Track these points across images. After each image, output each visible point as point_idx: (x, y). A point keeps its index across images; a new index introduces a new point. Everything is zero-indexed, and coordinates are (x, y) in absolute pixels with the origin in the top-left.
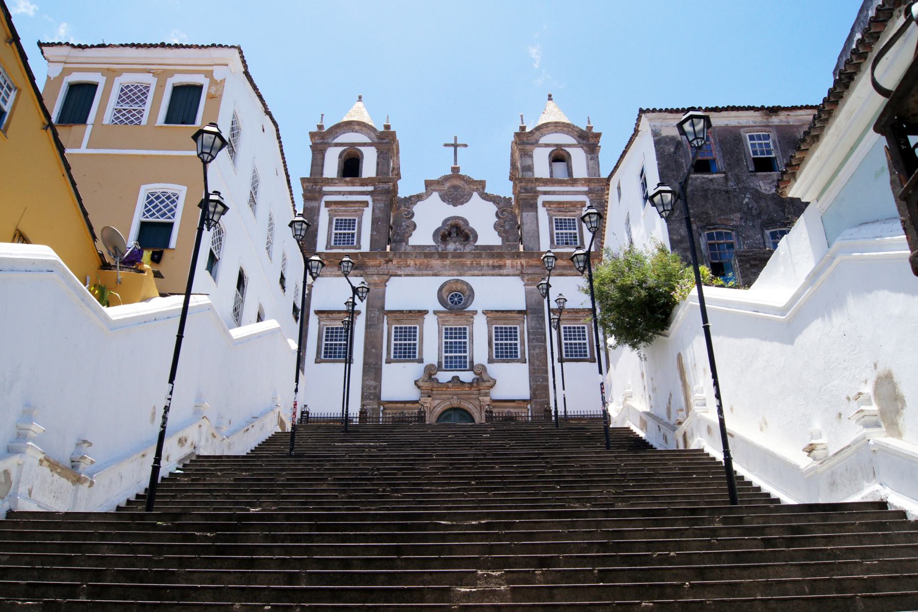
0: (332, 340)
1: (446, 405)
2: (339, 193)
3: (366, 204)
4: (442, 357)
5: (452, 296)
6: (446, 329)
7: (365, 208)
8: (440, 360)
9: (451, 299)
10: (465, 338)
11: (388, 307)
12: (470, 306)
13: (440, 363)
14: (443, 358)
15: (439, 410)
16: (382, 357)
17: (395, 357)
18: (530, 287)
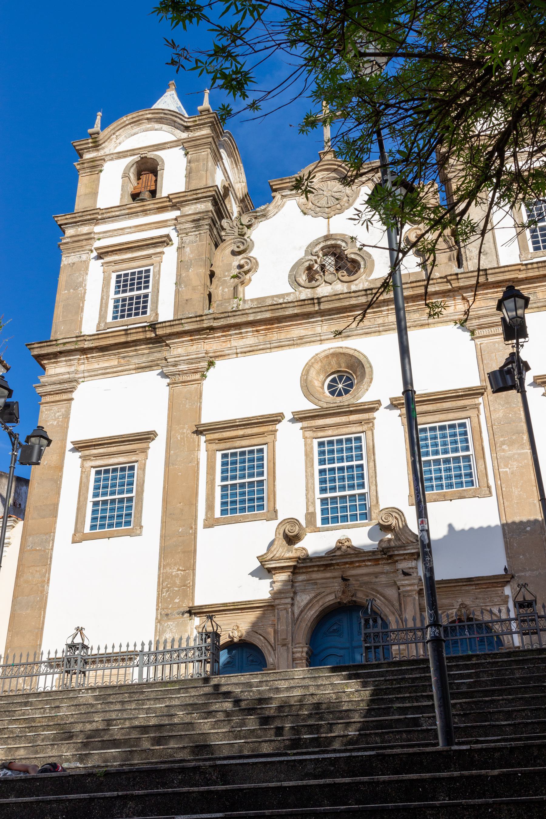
0: (105, 494)
1: (330, 599)
2: (122, 231)
3: (165, 241)
4: (314, 503)
5: (333, 380)
6: (321, 444)
7: (166, 250)
8: (311, 510)
9: (330, 387)
10: (360, 457)
11: (207, 418)
12: (368, 393)
13: (310, 516)
14: (318, 503)
15: (312, 613)
16: (196, 516)
17: (224, 512)
18: (485, 341)
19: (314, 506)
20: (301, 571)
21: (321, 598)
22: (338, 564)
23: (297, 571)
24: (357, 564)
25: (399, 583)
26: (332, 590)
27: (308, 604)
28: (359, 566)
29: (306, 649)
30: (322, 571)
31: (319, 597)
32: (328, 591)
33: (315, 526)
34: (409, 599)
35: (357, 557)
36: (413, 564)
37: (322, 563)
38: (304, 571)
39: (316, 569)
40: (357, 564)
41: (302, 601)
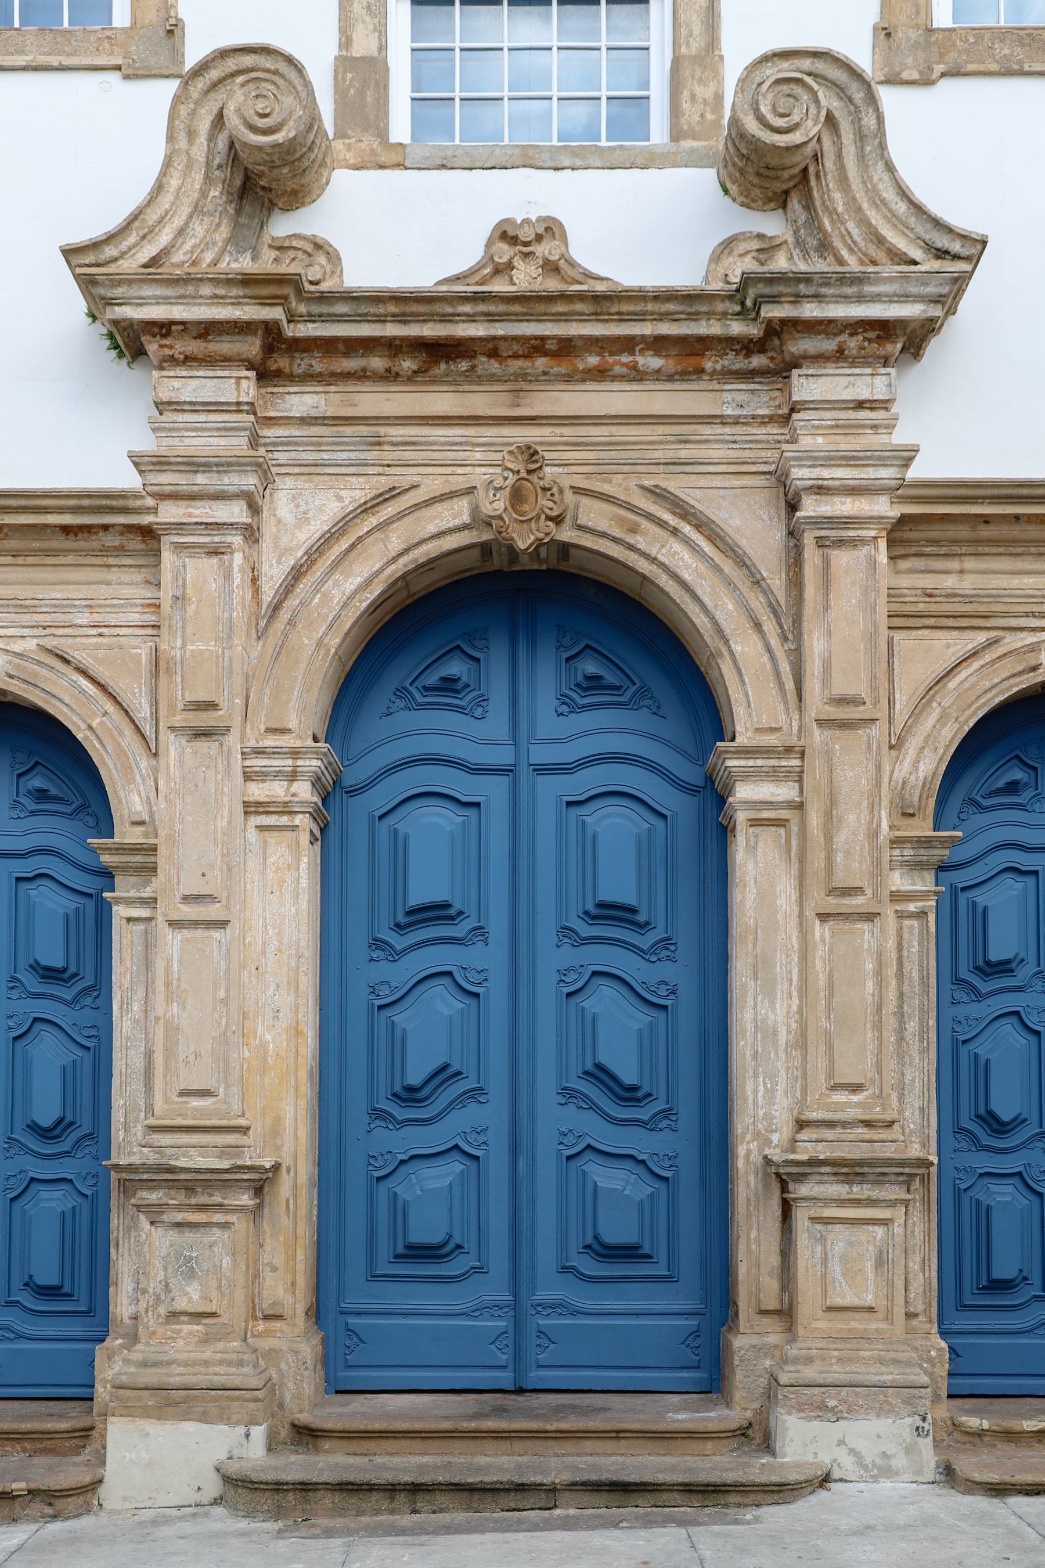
19: (381, 31)
20: (301, 364)
21: (401, 516)
22: (493, 348)
23: (282, 362)
24: (593, 360)
25: (801, 474)
26: (459, 483)
27: (329, 538)
28: (601, 374)
29: (312, 764)
30: (412, 378)
31: (388, 510)
32: (433, 484)
33: (382, 134)
34: (841, 558)
35: (597, 316)
36: (880, 382)
37: (414, 330)
38: (318, 365)
39: (377, 363)
40: (593, 360)
41: (304, 519)
